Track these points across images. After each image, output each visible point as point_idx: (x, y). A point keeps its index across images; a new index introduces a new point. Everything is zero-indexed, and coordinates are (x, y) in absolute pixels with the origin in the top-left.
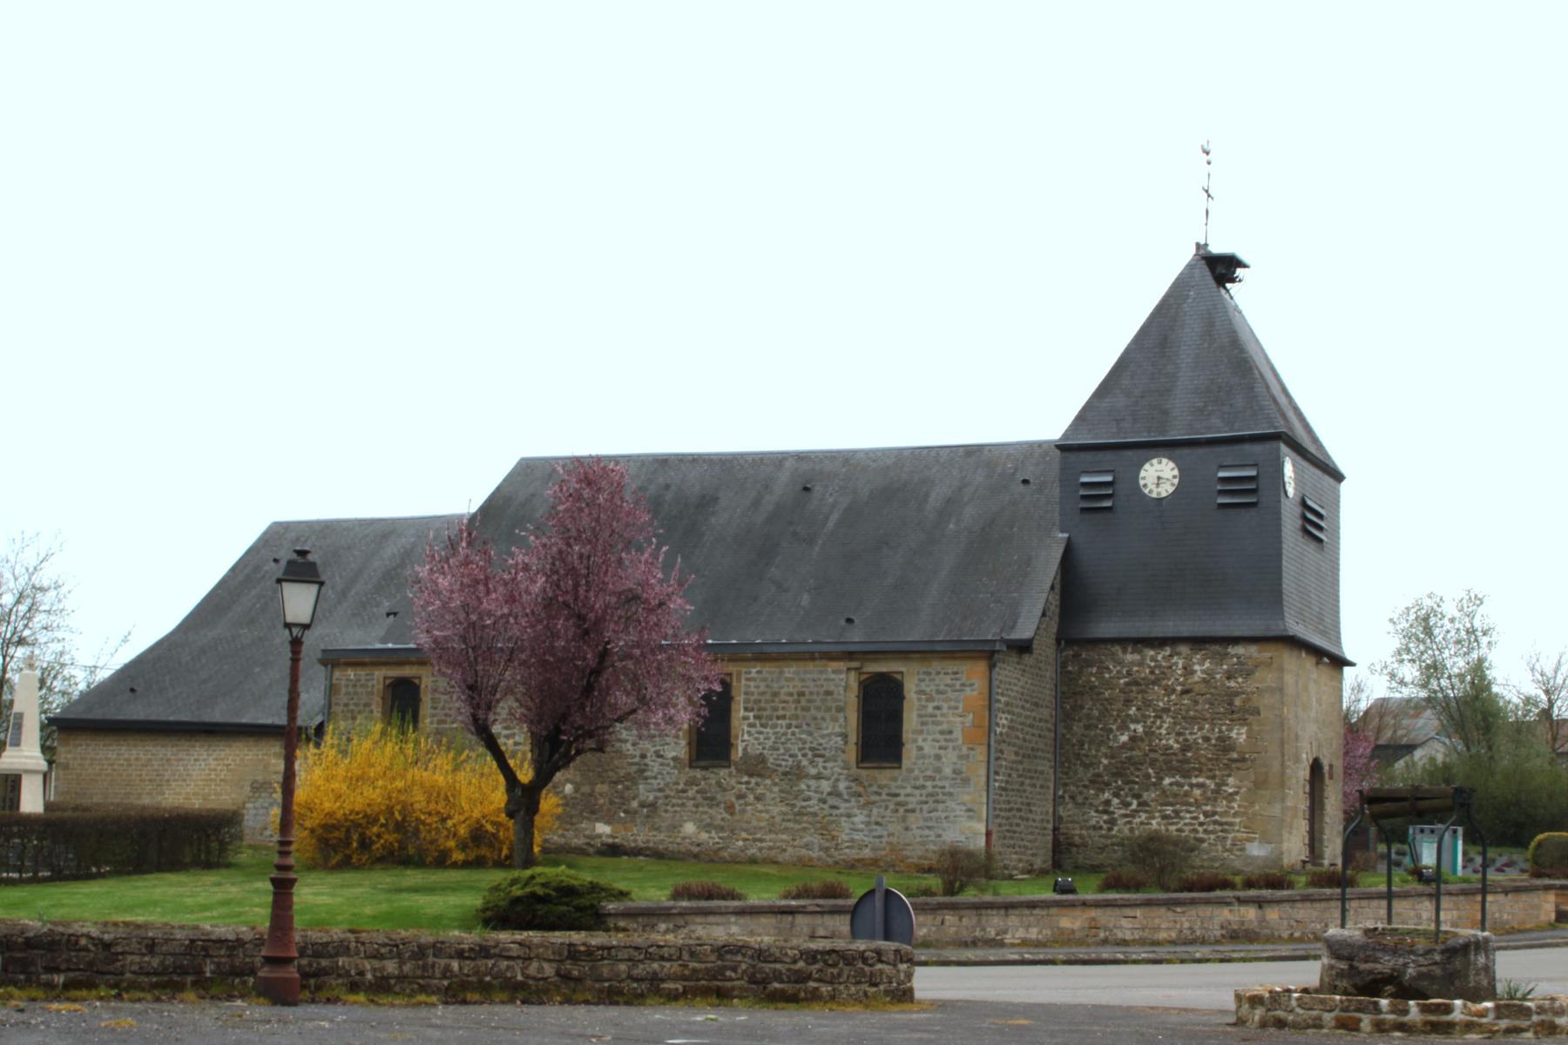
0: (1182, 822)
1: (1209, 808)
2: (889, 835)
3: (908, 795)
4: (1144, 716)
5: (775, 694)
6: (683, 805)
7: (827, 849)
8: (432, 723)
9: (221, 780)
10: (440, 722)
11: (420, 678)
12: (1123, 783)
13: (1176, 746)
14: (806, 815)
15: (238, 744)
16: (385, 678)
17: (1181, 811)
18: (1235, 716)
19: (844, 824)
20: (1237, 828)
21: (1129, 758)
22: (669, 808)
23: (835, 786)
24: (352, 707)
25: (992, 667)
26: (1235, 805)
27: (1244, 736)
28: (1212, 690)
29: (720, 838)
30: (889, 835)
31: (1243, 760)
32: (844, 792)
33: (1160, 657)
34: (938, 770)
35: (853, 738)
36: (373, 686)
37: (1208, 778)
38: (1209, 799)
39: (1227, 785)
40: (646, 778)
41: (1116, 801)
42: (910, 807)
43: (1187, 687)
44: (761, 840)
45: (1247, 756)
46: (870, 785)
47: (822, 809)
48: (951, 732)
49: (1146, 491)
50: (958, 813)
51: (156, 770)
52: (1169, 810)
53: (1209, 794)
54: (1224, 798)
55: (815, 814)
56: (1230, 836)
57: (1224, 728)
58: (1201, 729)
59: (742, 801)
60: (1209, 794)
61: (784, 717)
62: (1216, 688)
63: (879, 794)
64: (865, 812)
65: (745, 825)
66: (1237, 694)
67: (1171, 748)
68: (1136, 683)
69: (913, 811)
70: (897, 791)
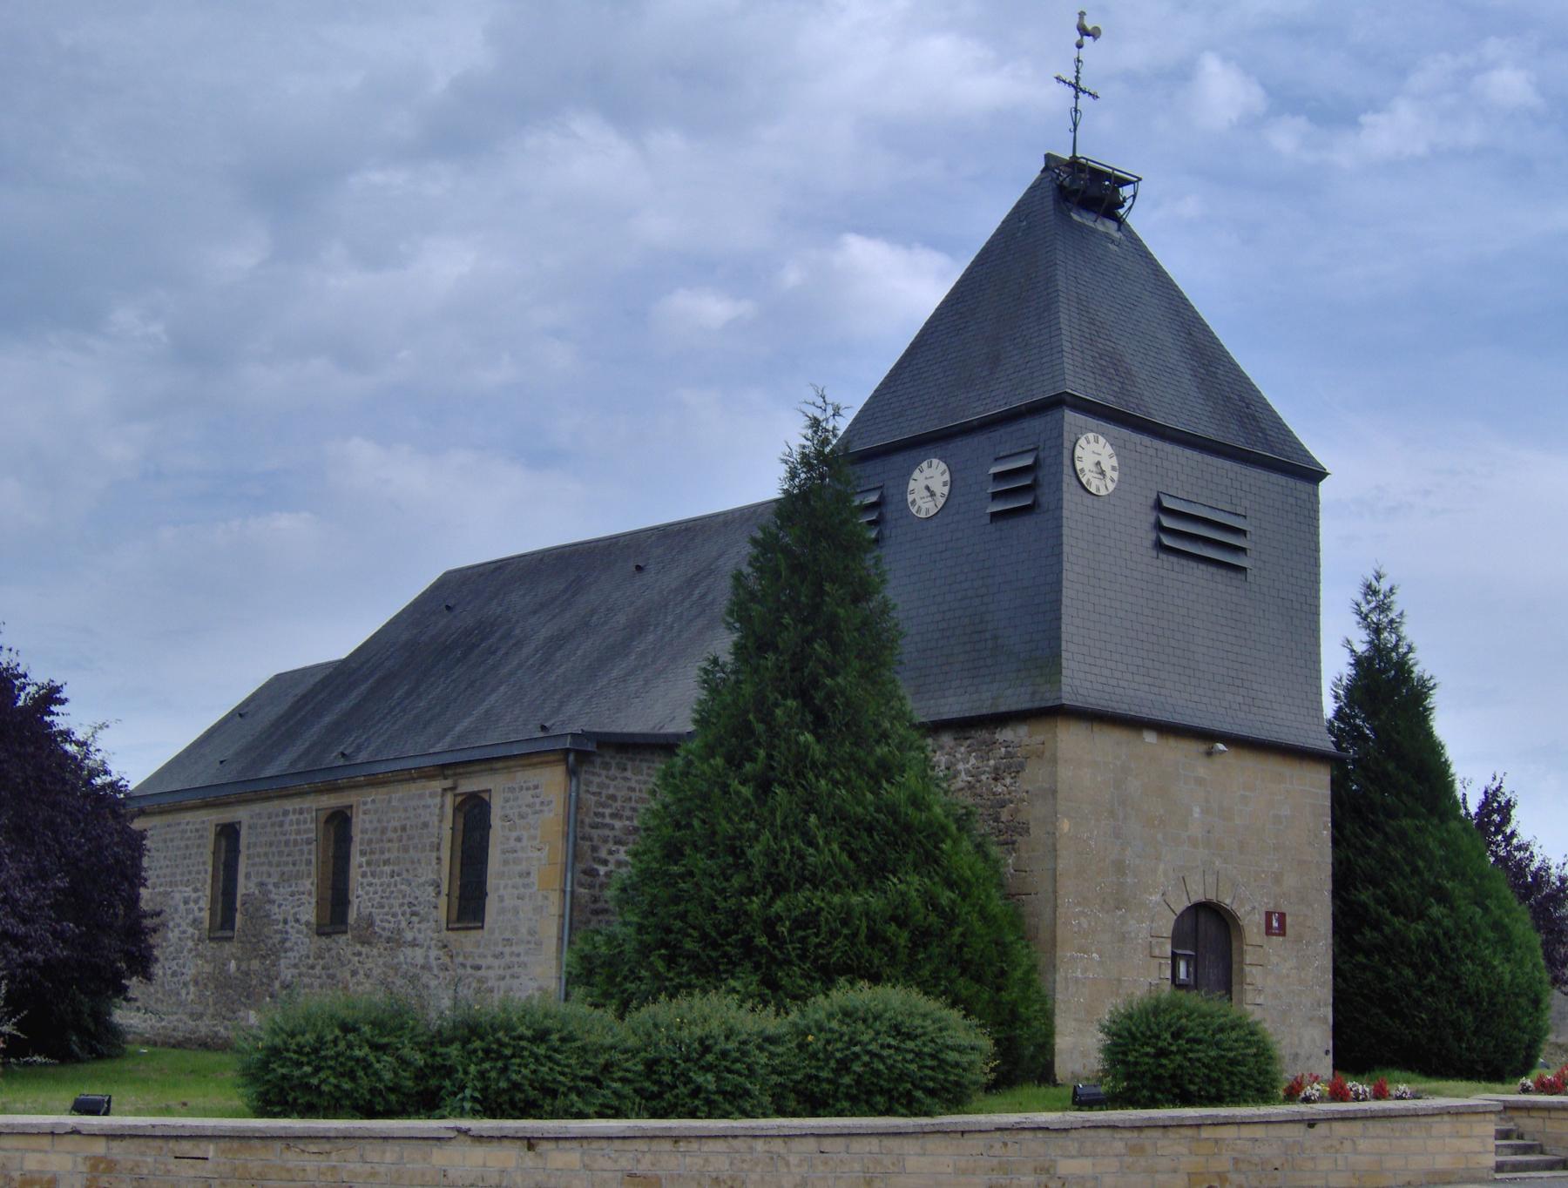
5: (384, 830)
25: (572, 773)
32: (434, 963)
34: (516, 930)
35: (445, 889)
48: (528, 874)
49: (914, 511)
61: (386, 862)
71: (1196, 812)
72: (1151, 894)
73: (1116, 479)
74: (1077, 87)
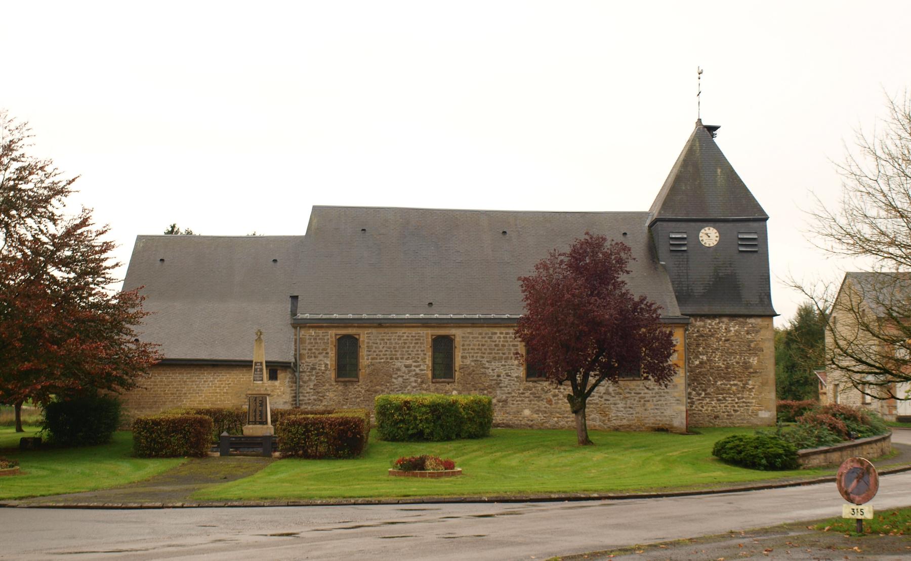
0: (727, 402)
1: (740, 395)
2: (636, 413)
3: (646, 393)
4: (707, 352)
6: (522, 400)
7: (604, 421)
8: (368, 359)
9: (224, 393)
10: (372, 359)
11: (359, 335)
12: (698, 384)
13: (723, 366)
14: (592, 404)
15: (235, 372)
16: (336, 335)
17: (726, 397)
18: (752, 352)
19: (612, 408)
20: (754, 404)
21: (700, 372)
22: (514, 402)
23: (607, 390)
24: (314, 351)
26: (752, 394)
27: (756, 361)
28: (740, 340)
29: (544, 417)
30: (636, 413)
31: (756, 372)
33: (713, 324)
36: (328, 339)
37: (739, 381)
38: (739, 391)
39: (748, 384)
40: (501, 387)
41: (694, 393)
42: (647, 399)
43: (727, 338)
44: (567, 417)
45: (758, 371)
46: (626, 389)
47: (601, 401)
49: (703, 243)
50: (672, 401)
51: (175, 388)
52: (720, 397)
53: (740, 389)
54: (747, 391)
55: (597, 404)
56: (751, 408)
57: (746, 358)
58: (735, 358)
59: (556, 398)
60: (740, 389)
62: (741, 338)
63: (630, 393)
64: (624, 402)
65: (558, 410)
66: (752, 342)
67: (721, 367)
68: (702, 336)
69: (648, 401)
70: (640, 391)
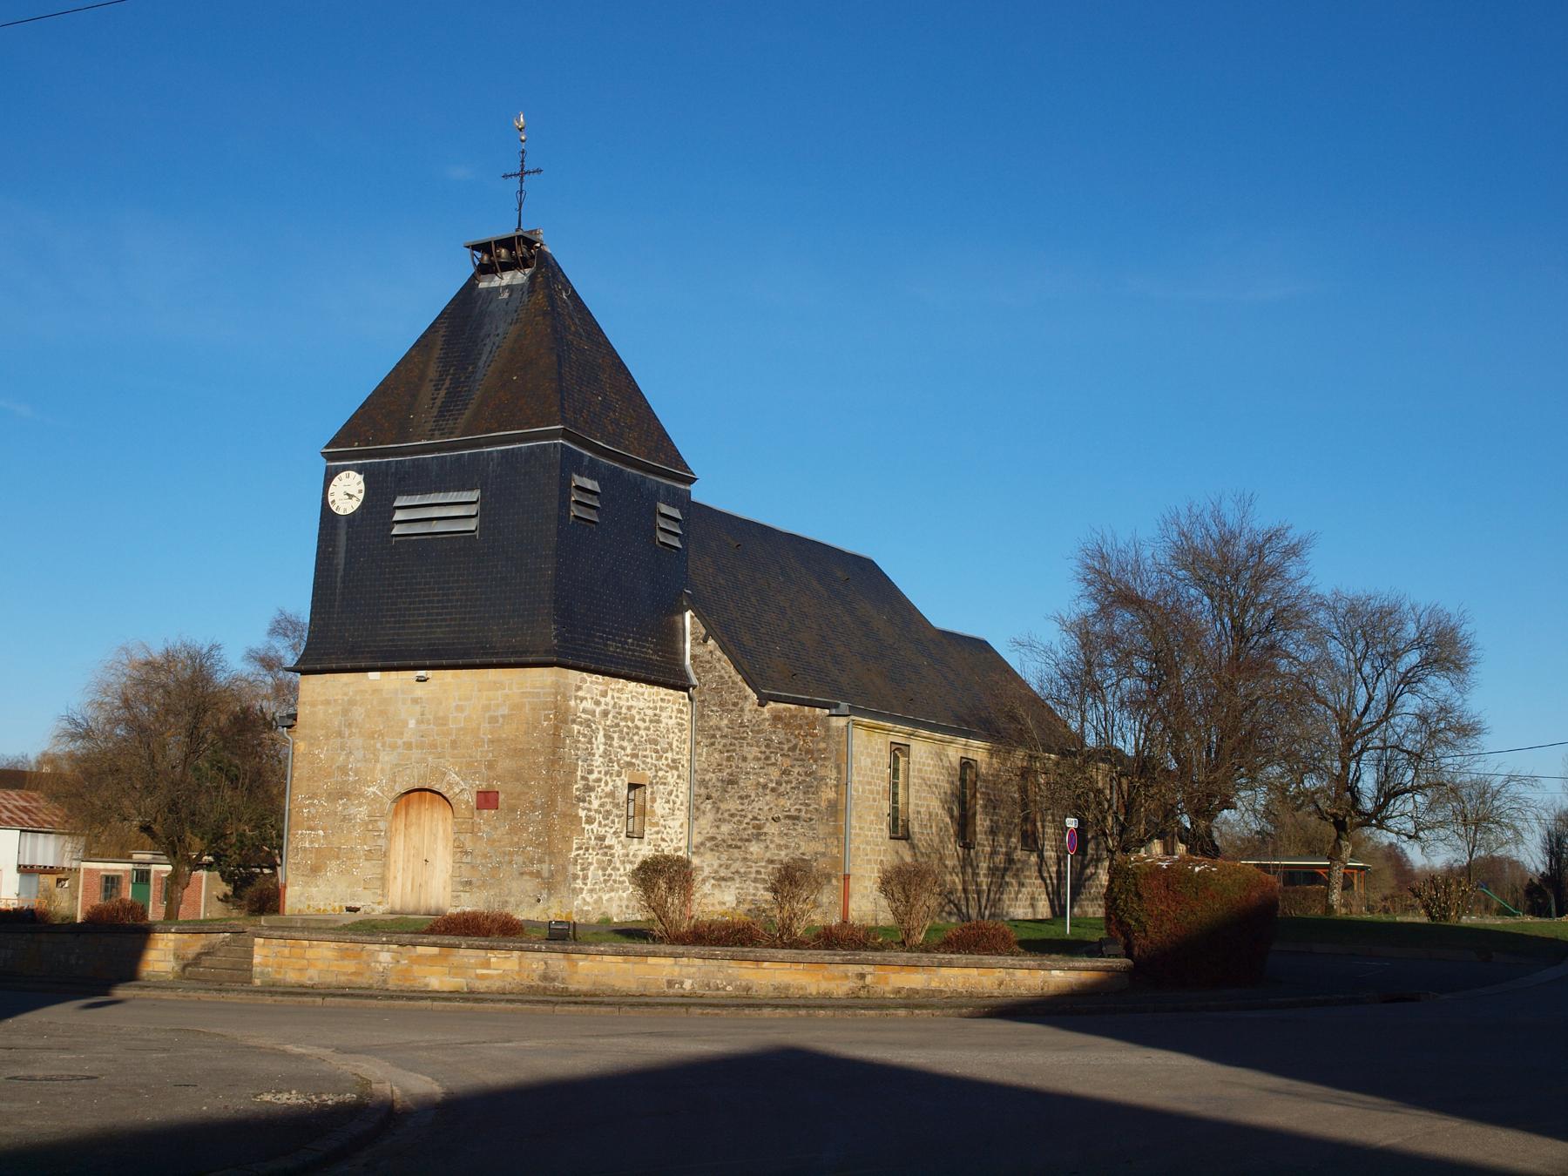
71: (412, 724)
72: (369, 787)
73: (361, 500)
74: (522, 174)
